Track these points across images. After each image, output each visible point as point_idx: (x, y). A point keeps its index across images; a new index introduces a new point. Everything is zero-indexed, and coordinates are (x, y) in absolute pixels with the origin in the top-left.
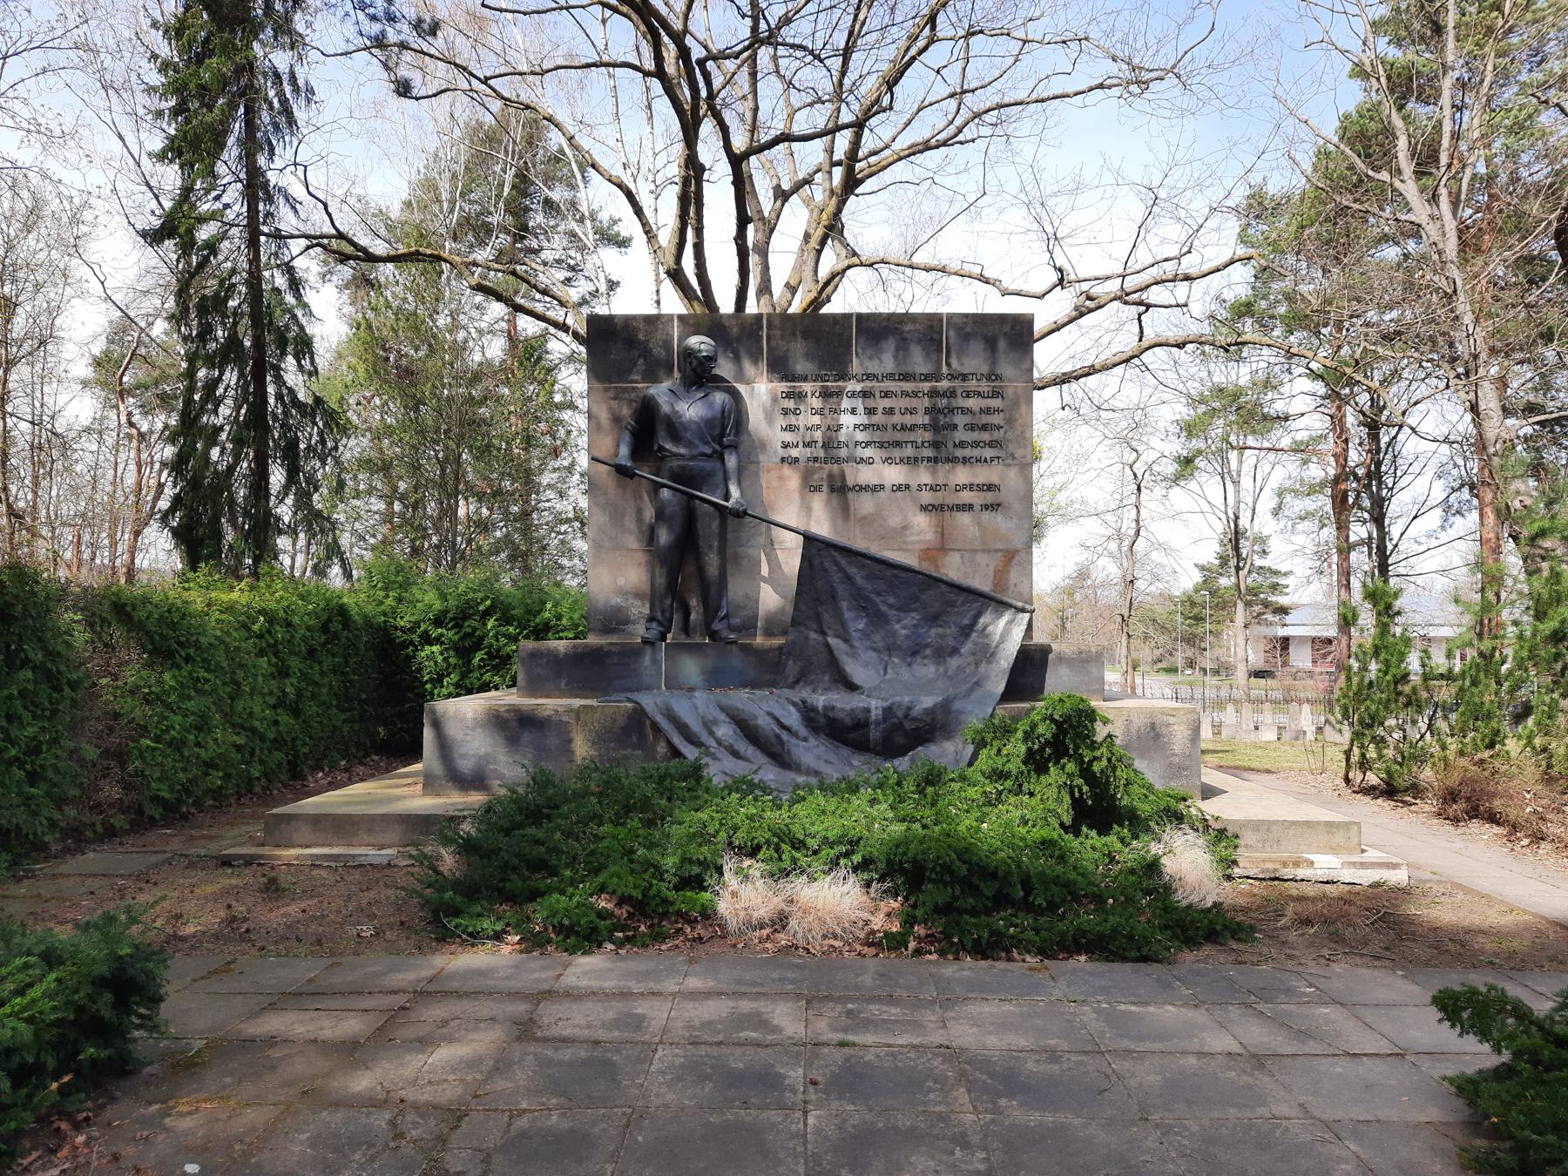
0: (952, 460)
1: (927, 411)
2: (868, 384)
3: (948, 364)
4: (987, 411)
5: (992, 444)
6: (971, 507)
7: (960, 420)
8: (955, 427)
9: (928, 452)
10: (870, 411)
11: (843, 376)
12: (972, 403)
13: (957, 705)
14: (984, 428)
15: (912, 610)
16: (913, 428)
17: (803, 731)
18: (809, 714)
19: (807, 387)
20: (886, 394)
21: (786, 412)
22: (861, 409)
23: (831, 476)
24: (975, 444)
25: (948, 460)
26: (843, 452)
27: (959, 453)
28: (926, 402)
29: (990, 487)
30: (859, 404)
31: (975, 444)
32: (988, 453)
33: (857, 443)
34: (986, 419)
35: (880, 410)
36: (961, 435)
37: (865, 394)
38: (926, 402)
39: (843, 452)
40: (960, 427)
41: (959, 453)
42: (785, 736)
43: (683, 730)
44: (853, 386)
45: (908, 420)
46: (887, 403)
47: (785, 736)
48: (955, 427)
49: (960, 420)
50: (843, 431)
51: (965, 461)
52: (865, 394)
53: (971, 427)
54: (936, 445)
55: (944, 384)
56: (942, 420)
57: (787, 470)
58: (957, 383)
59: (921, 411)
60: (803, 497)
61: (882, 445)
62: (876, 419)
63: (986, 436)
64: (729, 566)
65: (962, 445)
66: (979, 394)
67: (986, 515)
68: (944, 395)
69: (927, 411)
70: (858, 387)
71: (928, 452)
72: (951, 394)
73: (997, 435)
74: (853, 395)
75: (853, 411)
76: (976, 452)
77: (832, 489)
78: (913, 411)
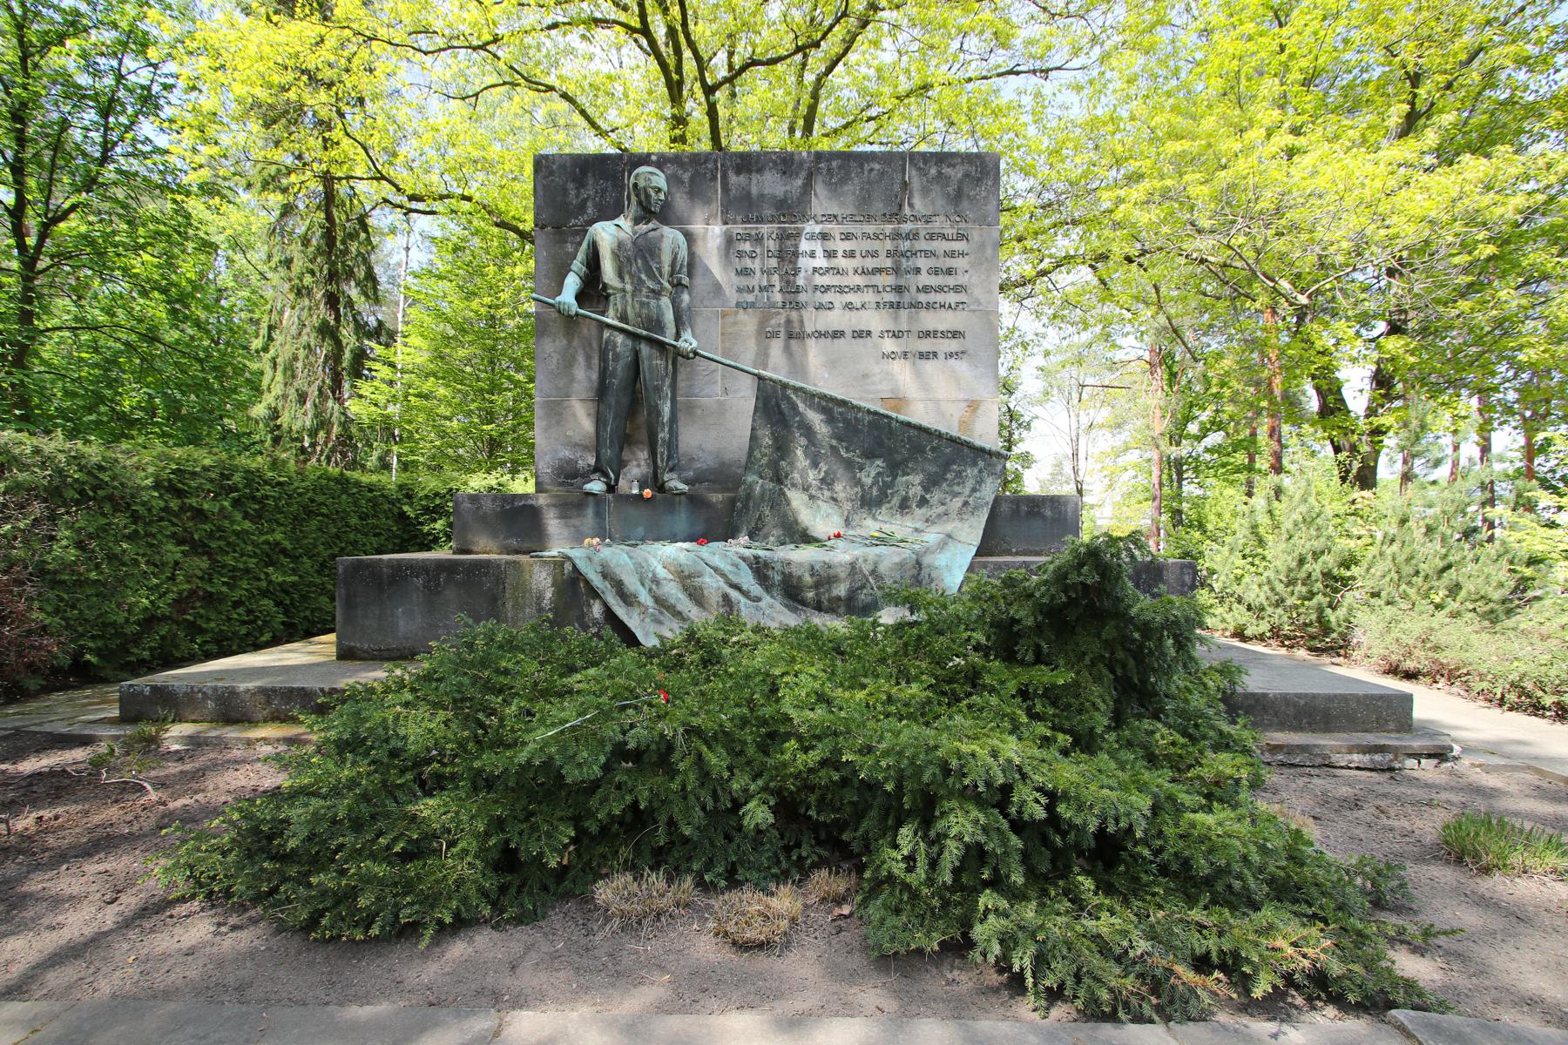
0: (916, 305)
1: (889, 254)
2: (828, 227)
3: (911, 205)
4: (951, 254)
5: (957, 289)
6: (935, 354)
7: (922, 263)
8: (918, 271)
9: (890, 297)
10: (830, 254)
11: (804, 218)
12: (940, 246)
13: (926, 561)
14: (949, 272)
15: (879, 457)
16: (879, 271)
17: (756, 590)
18: (760, 569)
19: (765, 229)
20: (847, 237)
21: (740, 254)
22: (820, 253)
23: (789, 322)
24: (940, 289)
25: (912, 306)
26: (802, 297)
27: (923, 298)
28: (889, 245)
29: (956, 334)
30: (818, 247)
31: (940, 289)
32: (952, 298)
33: (816, 288)
34: (950, 262)
35: (840, 254)
36: (925, 279)
37: (825, 236)
38: (889, 245)
39: (802, 297)
40: (924, 271)
41: (923, 298)
42: (734, 594)
43: (619, 587)
44: (811, 227)
45: (870, 263)
46: (848, 246)
47: (734, 594)
48: (918, 271)
49: (922, 263)
50: (802, 274)
51: (929, 306)
52: (825, 236)
53: (936, 271)
54: (899, 289)
55: (907, 227)
56: (904, 263)
57: (742, 316)
58: (919, 225)
59: (883, 254)
60: (759, 343)
61: (841, 290)
62: (835, 263)
63: (951, 281)
64: (681, 417)
65: (926, 289)
66: (944, 237)
67: (952, 361)
68: (907, 237)
69: (889, 254)
70: (818, 229)
71: (890, 297)
72: (914, 236)
73: (961, 279)
74: (812, 237)
75: (812, 255)
76: (940, 298)
77: (790, 336)
78: (874, 254)
